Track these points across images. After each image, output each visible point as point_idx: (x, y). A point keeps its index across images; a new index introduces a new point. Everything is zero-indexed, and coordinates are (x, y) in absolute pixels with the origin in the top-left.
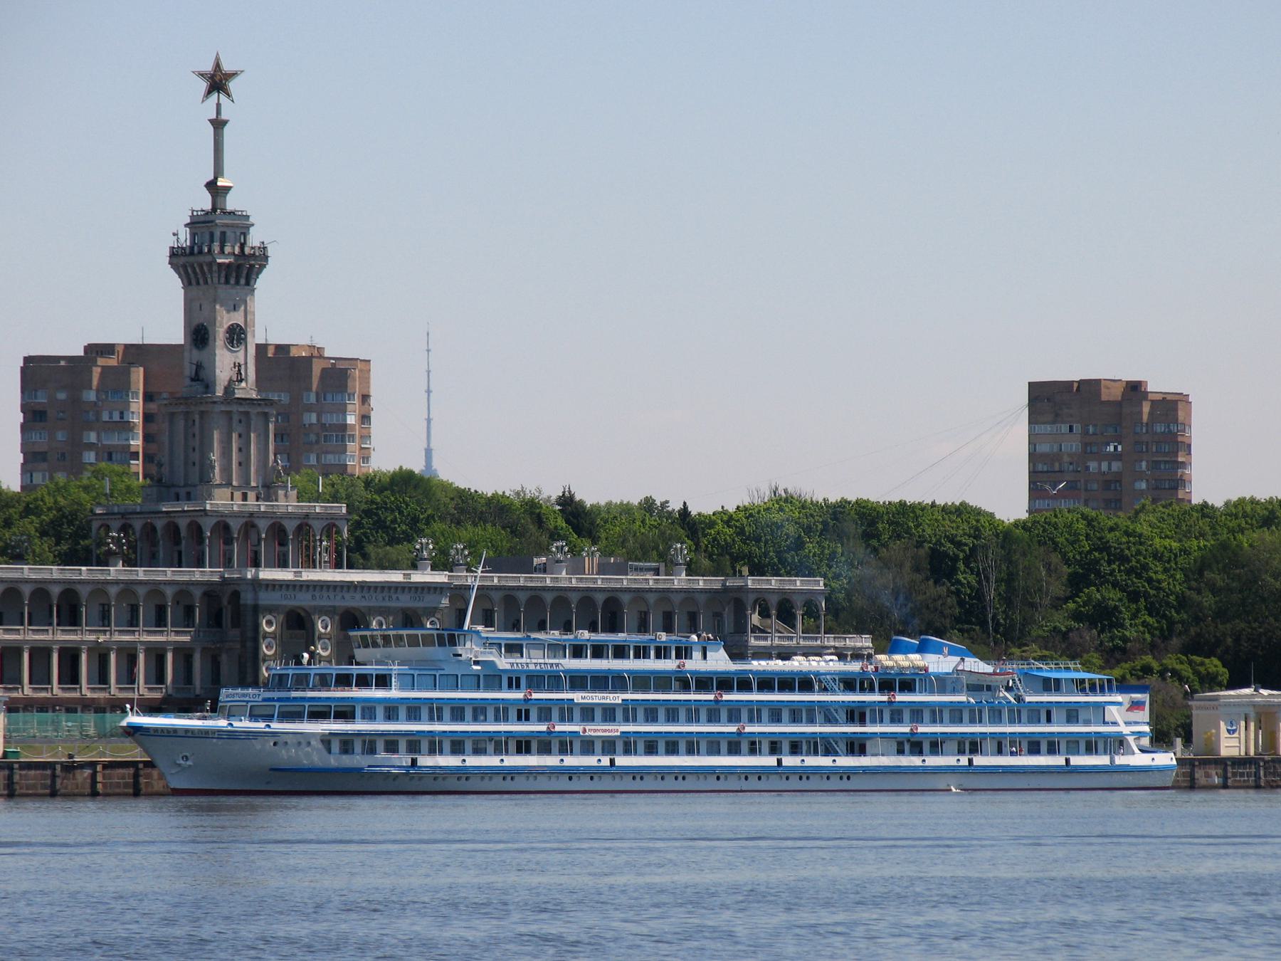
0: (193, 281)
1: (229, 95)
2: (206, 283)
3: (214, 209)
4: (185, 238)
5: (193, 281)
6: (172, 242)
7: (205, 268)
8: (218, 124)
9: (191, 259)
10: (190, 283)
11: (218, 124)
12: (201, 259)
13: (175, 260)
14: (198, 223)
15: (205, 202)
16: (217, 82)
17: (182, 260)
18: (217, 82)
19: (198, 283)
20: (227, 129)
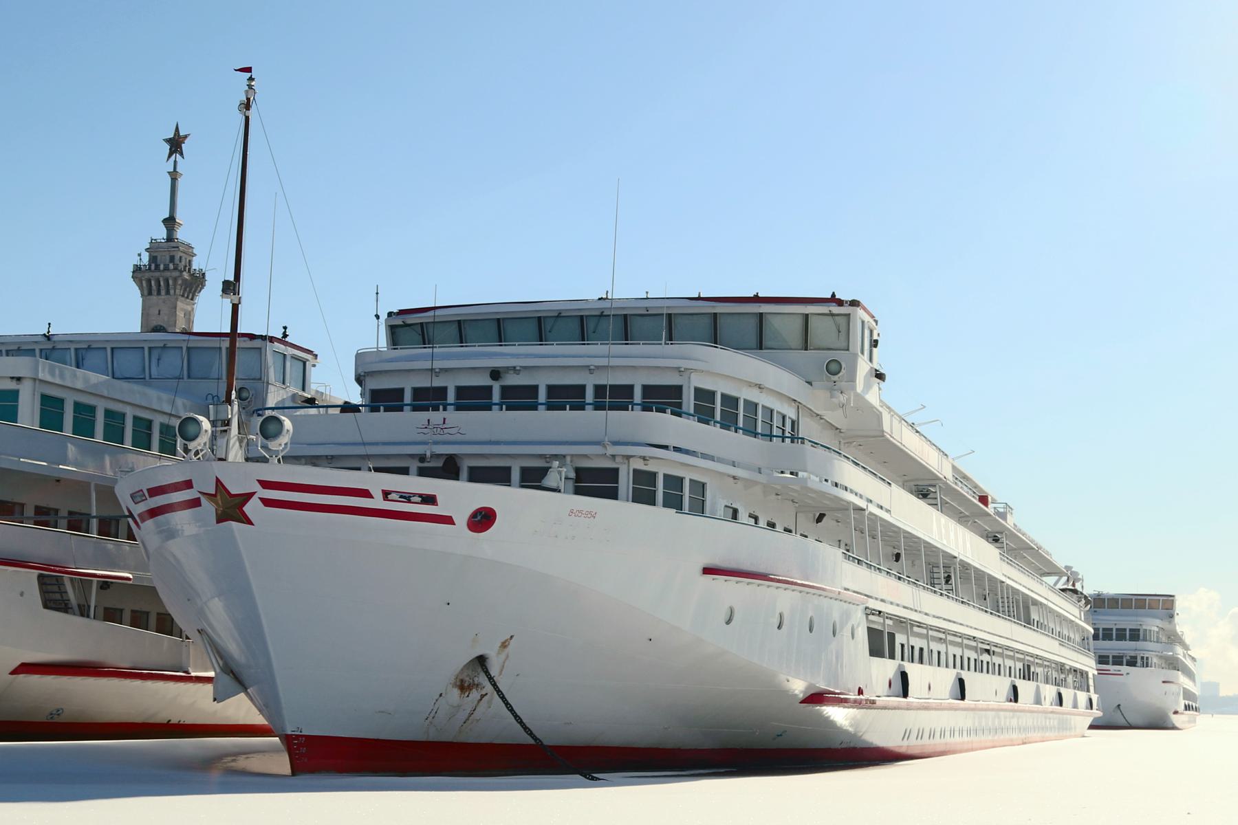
0: (155, 292)
1: (181, 154)
2: (168, 293)
3: (170, 238)
4: (146, 259)
5: (155, 292)
6: (136, 261)
7: (171, 282)
8: (174, 176)
9: (157, 274)
10: (150, 293)
11: (174, 176)
12: (167, 274)
13: (139, 275)
14: (153, 248)
15: (161, 233)
16: (176, 144)
17: (147, 275)
18: (176, 144)
19: (159, 293)
20: (181, 182)
